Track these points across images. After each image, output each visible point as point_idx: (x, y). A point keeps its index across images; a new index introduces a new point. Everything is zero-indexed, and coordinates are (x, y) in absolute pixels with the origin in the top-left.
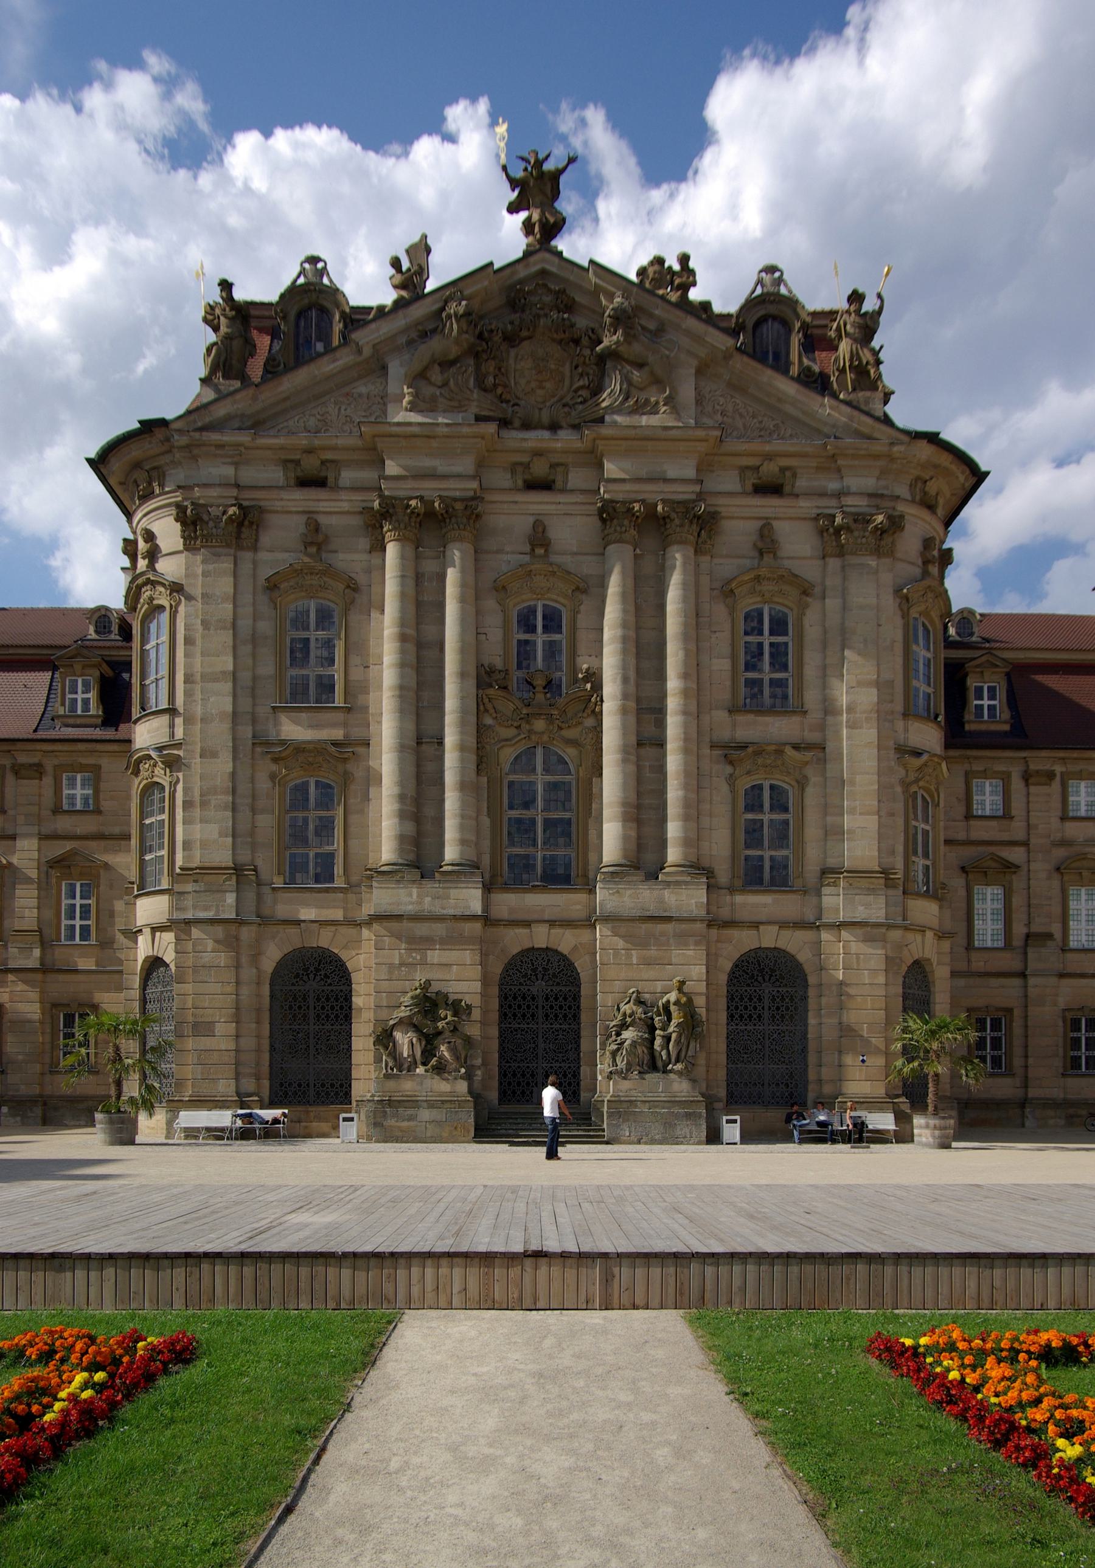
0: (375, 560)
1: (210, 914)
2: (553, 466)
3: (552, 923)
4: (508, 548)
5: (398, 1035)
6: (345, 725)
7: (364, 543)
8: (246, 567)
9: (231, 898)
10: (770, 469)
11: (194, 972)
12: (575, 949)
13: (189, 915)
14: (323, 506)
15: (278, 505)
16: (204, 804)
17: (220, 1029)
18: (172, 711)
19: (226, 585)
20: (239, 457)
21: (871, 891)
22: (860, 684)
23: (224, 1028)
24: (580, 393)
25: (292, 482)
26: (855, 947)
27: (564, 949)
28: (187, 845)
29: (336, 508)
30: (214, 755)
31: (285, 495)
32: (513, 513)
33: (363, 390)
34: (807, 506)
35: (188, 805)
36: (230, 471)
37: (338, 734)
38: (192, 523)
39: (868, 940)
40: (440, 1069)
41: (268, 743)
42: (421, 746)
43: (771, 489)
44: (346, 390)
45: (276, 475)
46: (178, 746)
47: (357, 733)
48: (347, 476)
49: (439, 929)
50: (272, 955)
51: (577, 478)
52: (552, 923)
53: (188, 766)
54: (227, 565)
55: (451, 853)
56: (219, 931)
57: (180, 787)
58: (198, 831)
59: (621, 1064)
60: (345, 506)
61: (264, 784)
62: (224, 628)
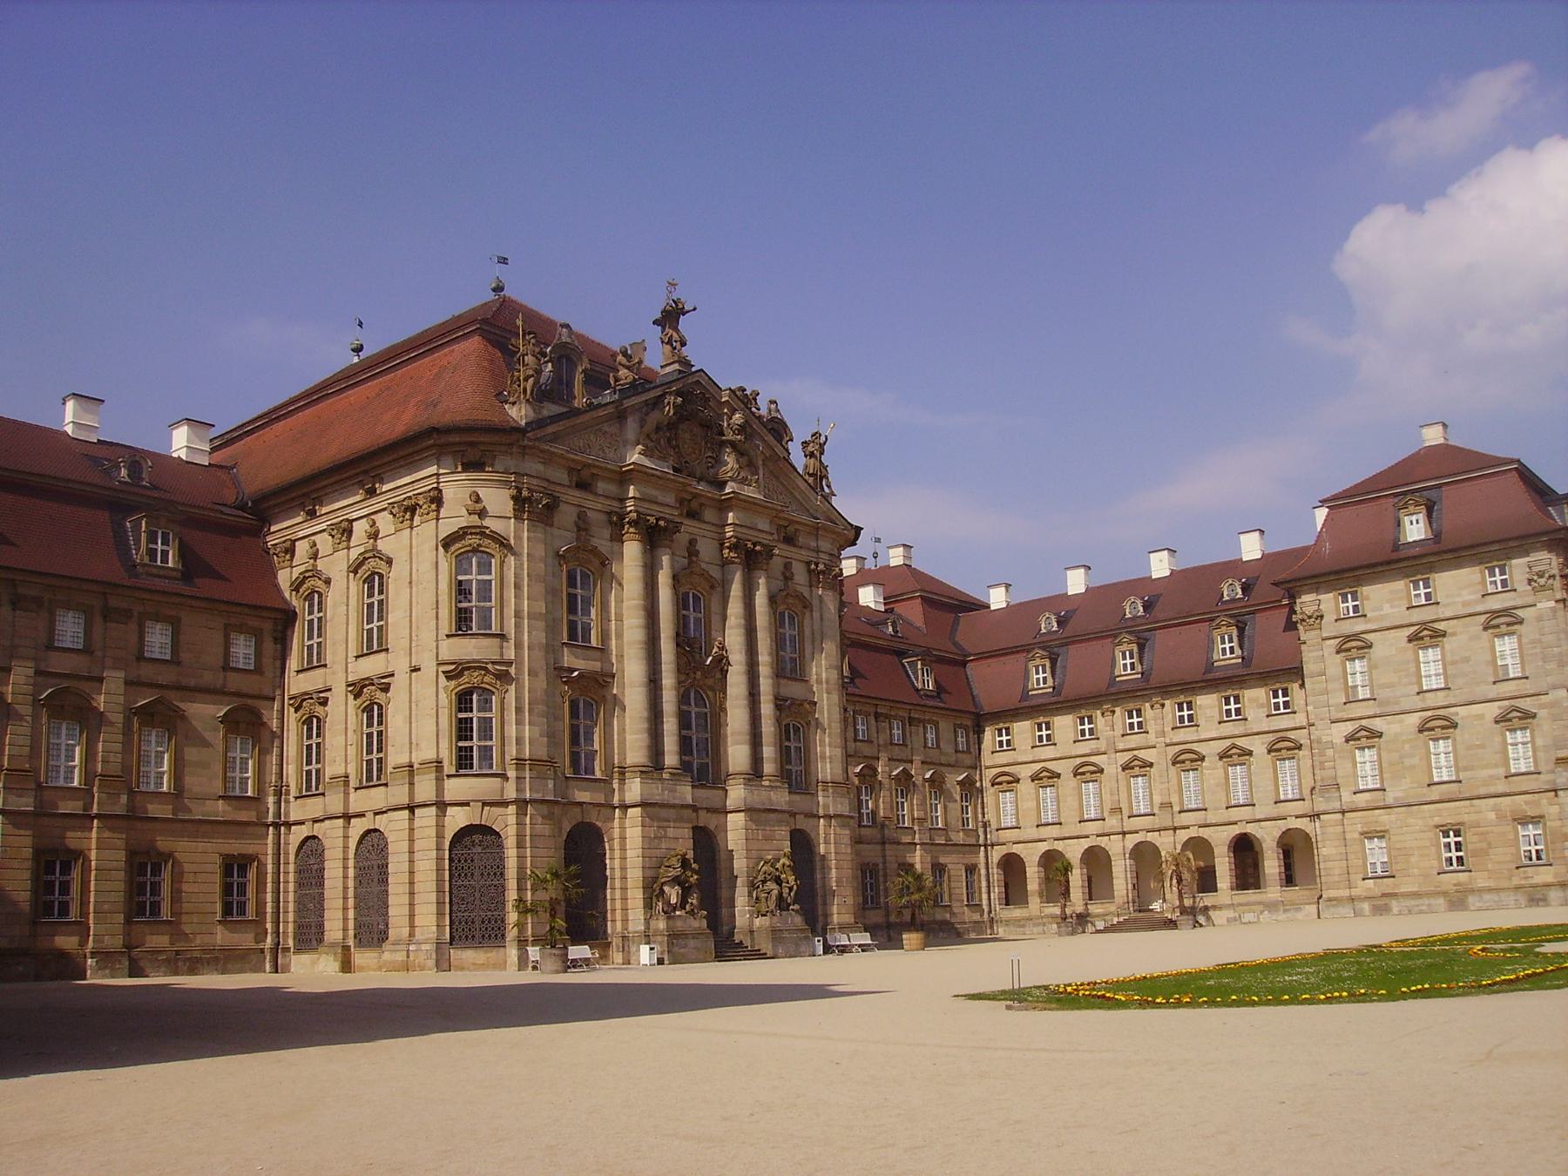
0: (616, 546)
2: (702, 505)
3: (708, 810)
5: (666, 888)
6: (601, 660)
7: (607, 533)
9: (551, 784)
10: (791, 529)
14: (588, 504)
18: (502, 637)
19: (540, 550)
20: (548, 459)
26: (838, 830)
27: (712, 827)
28: (519, 741)
29: (595, 506)
30: (536, 675)
31: (571, 492)
34: (805, 555)
36: (541, 467)
37: (596, 666)
39: (843, 826)
40: (692, 913)
41: (561, 669)
43: (789, 540)
45: (561, 476)
46: (510, 664)
48: (601, 486)
49: (671, 813)
50: (567, 827)
51: (709, 515)
52: (708, 810)
56: (544, 809)
59: (772, 906)
60: (599, 507)
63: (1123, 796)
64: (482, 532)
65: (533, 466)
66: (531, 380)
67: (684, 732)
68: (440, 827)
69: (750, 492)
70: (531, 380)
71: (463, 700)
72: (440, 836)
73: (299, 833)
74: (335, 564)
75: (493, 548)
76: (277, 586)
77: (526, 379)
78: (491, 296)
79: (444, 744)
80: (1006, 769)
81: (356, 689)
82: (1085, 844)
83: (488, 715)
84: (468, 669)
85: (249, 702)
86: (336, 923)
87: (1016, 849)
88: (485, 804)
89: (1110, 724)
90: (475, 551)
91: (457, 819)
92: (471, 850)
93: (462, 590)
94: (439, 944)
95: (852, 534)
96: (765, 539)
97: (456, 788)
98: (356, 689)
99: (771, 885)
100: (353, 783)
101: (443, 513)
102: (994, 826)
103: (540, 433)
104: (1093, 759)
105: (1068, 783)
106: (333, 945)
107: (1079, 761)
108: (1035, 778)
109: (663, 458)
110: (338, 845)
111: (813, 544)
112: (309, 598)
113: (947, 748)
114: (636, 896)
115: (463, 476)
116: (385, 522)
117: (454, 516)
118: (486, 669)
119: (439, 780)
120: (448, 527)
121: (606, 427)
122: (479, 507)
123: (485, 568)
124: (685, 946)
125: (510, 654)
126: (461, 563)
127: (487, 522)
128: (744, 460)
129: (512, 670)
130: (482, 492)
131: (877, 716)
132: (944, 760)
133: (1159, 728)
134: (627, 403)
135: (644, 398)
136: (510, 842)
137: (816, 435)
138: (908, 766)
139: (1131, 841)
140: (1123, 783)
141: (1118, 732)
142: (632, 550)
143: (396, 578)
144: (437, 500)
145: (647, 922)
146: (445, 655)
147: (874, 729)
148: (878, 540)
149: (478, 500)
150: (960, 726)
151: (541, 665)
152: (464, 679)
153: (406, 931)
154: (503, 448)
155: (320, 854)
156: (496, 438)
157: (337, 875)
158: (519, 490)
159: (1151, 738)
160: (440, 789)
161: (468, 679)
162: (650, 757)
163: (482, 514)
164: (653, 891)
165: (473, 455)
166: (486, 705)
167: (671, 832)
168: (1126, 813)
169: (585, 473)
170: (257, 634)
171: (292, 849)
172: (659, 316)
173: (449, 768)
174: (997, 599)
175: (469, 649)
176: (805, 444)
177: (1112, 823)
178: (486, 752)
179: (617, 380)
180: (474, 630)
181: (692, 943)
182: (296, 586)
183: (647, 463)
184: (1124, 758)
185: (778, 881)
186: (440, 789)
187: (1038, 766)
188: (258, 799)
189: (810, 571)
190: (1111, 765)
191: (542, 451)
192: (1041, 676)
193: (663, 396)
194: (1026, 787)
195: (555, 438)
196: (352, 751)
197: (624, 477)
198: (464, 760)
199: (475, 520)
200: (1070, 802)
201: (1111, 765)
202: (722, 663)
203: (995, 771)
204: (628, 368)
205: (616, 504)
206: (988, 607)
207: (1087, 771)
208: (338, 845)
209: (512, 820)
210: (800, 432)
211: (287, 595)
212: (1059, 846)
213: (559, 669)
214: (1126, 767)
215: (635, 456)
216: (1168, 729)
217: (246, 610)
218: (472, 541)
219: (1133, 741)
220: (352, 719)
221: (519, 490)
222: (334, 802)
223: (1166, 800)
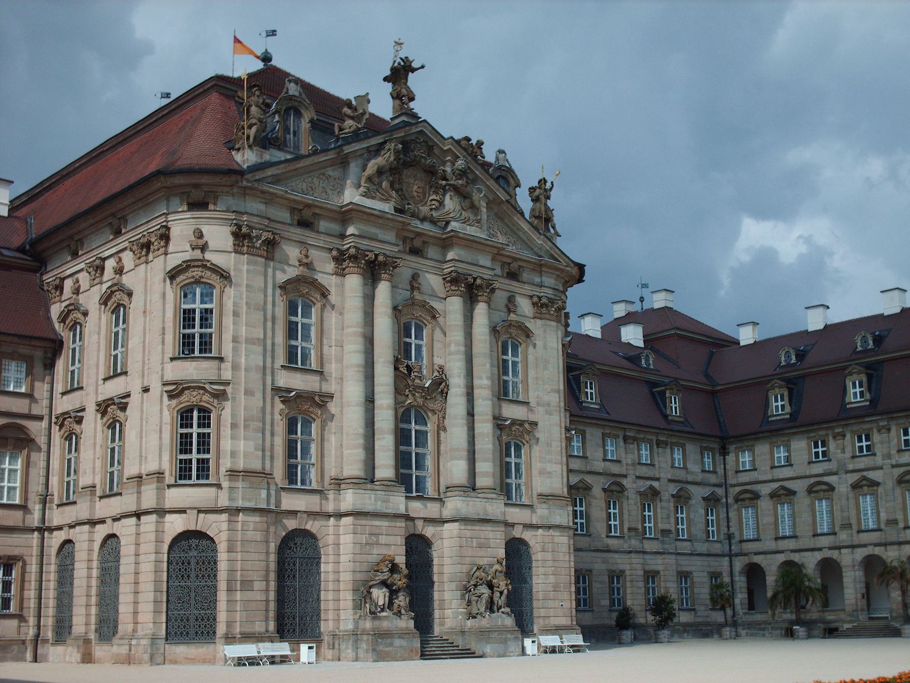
1: (251, 505)
2: (424, 243)
4: (400, 286)
7: (331, 266)
8: (270, 271)
9: (264, 494)
10: (515, 265)
11: (242, 545)
12: (433, 535)
13: (240, 503)
15: (286, 235)
16: (246, 427)
17: (258, 585)
20: (270, 199)
21: (562, 507)
22: (553, 391)
23: (259, 585)
24: (433, 202)
25: (296, 223)
31: (292, 229)
32: (408, 265)
33: (331, 173)
34: (528, 289)
35: (234, 426)
36: (262, 207)
38: (241, 237)
40: (399, 614)
42: (370, 400)
43: (513, 276)
44: (323, 171)
47: (326, 388)
48: (323, 225)
49: (384, 523)
51: (432, 252)
53: (234, 399)
54: (262, 269)
55: (380, 473)
57: (227, 414)
58: (242, 445)
59: (483, 609)
61: (277, 417)
62: (258, 309)
63: (853, 513)
64: (204, 265)
65: (255, 205)
66: (254, 129)
67: (402, 448)
68: (159, 532)
69: (472, 231)
70: (254, 129)
71: (185, 417)
72: (159, 541)
73: (58, 537)
74: (91, 299)
75: (214, 279)
76: (49, 318)
77: (250, 127)
78: (260, 65)
79: (166, 457)
80: (749, 487)
81: (103, 407)
82: (818, 556)
83: (206, 430)
84: (188, 388)
85: (19, 421)
86: (83, 618)
87: (757, 559)
88: (199, 512)
89: (843, 449)
90: (198, 282)
91: (175, 525)
92: (191, 555)
93: (188, 317)
94: (154, 639)
95: (575, 271)
96: (487, 274)
97: (176, 497)
98: (103, 407)
99: (484, 590)
100: (99, 493)
101: (171, 248)
102: (737, 537)
103: (259, 175)
104: (826, 479)
105: (802, 501)
106: (77, 638)
107: (813, 480)
108: (773, 495)
109: (386, 200)
110: (87, 545)
111: (537, 280)
112: (73, 328)
113: (694, 467)
114: (347, 598)
115: (188, 215)
116: (128, 259)
117: (180, 250)
118: (203, 388)
119: (160, 491)
120: (174, 261)
121: (330, 172)
122: (201, 242)
123: (207, 296)
124: (391, 645)
125: (227, 375)
126: (186, 293)
127: (208, 256)
128: (467, 203)
129: (229, 390)
130: (205, 229)
131: (625, 439)
132: (690, 478)
133: (885, 451)
134: (347, 149)
135: (365, 145)
136: (222, 547)
137: (543, 181)
138: (656, 484)
139: (860, 554)
140: (852, 501)
141: (848, 454)
142: (354, 282)
143: (136, 305)
144: (165, 237)
145: (356, 622)
146: (170, 376)
147: (622, 450)
148: (645, 286)
149: (200, 235)
150: (706, 448)
151: (257, 386)
152: (184, 398)
153: (130, 627)
154: (227, 189)
155: (72, 555)
156: (216, 180)
157: (85, 574)
158: (239, 227)
159: (879, 460)
160: (160, 497)
161: (188, 399)
162: (366, 471)
163: (204, 248)
164: (363, 594)
165: (197, 195)
166: (205, 422)
167: (383, 539)
168: (855, 528)
169: (307, 213)
170: (29, 361)
171: (54, 551)
172: (388, 73)
173: (169, 479)
174: (746, 336)
175: (193, 370)
176: (532, 190)
177: (843, 537)
178: (203, 465)
179: (341, 129)
180: (197, 354)
181: (398, 642)
182: (63, 319)
183: (368, 203)
184: (853, 478)
185: (491, 586)
186: (160, 497)
187: (776, 485)
188: (23, 507)
189: (534, 304)
190: (842, 484)
191: (263, 192)
192: (780, 403)
193: (385, 142)
194: (765, 504)
195: (277, 180)
196: (98, 463)
197: (346, 215)
198: (184, 471)
199: (197, 254)
200: (805, 518)
201: (842, 484)
202: (440, 386)
203: (738, 489)
204: (352, 118)
205: (337, 241)
206: (737, 343)
207: (820, 489)
208: (87, 545)
209: (225, 526)
210: (527, 179)
211: (57, 325)
212: (796, 557)
213: (276, 390)
214: (855, 486)
215: (351, 196)
216: (894, 452)
217: (16, 340)
218: (196, 273)
219: (862, 463)
220: (99, 435)
221: (239, 227)
222: (81, 511)
223: (891, 517)
